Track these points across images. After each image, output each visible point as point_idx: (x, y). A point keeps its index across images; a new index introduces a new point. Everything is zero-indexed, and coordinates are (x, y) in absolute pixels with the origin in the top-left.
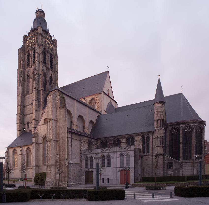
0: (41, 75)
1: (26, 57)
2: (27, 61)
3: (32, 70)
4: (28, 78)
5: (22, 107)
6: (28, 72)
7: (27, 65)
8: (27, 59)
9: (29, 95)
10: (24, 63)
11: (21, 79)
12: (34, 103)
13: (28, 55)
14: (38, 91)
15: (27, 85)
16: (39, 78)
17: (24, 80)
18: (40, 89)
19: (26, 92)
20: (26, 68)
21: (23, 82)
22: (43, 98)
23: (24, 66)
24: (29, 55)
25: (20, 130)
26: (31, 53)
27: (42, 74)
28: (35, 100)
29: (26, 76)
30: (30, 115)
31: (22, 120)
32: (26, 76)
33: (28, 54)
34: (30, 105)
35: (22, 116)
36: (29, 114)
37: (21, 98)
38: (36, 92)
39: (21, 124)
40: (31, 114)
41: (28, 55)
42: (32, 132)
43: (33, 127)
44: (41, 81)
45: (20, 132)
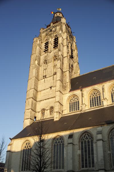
0: (66, 57)
1: (43, 45)
2: (45, 48)
3: (51, 55)
4: (44, 63)
5: (35, 91)
6: (45, 57)
7: (44, 51)
8: (45, 47)
9: (46, 79)
10: (41, 49)
11: (36, 62)
12: (58, 83)
13: (47, 44)
14: (63, 72)
15: (43, 69)
16: (63, 60)
17: (39, 64)
18: (66, 70)
19: (41, 76)
20: (42, 54)
21: (38, 66)
22: (69, 80)
23: (40, 52)
24: (48, 43)
25: (31, 118)
26: (51, 40)
27: (67, 56)
28: (60, 80)
29: (42, 61)
30: (47, 100)
31: (33, 106)
32: (42, 61)
33: (45, 43)
34: (47, 89)
35: (34, 102)
36: (45, 100)
37: (35, 81)
38: (61, 72)
39: (33, 110)
40: (48, 99)
41: (47, 44)
42: (55, 118)
43: (57, 112)
44: (66, 63)
45: (30, 120)
